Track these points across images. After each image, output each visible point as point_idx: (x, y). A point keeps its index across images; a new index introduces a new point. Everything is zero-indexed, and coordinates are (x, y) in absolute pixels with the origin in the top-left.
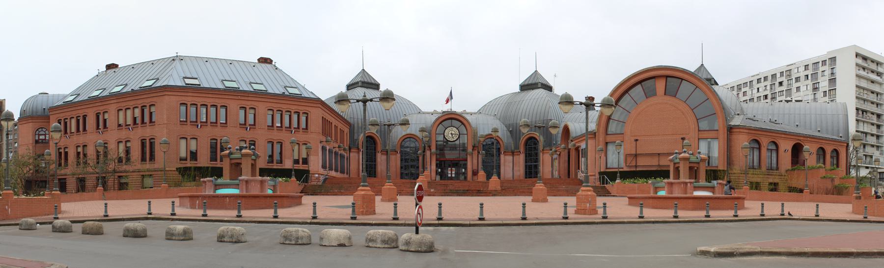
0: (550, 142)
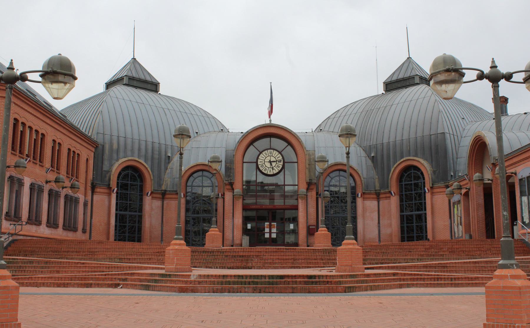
0: (443, 175)
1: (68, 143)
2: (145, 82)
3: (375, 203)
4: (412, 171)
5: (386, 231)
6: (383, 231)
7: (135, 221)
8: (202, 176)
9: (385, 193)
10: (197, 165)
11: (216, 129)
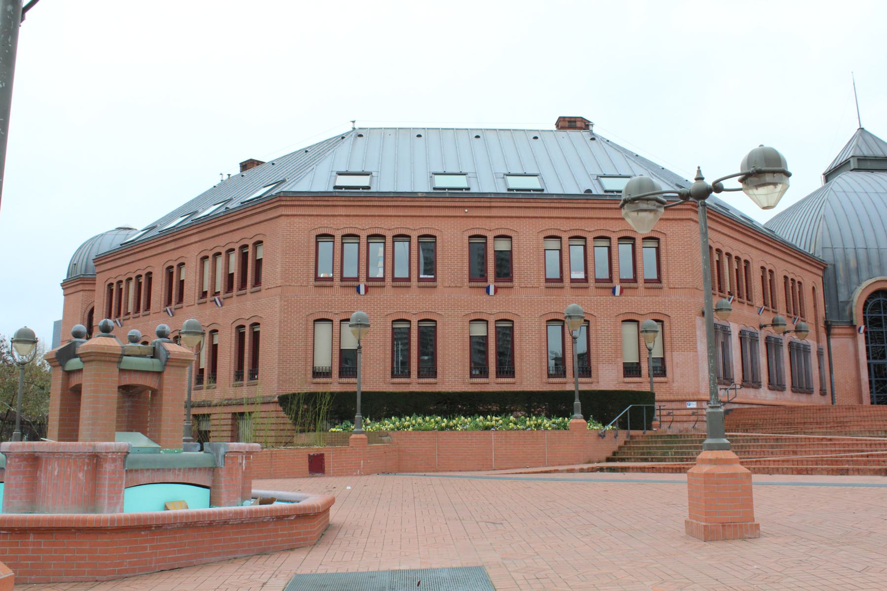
1: (782, 268)
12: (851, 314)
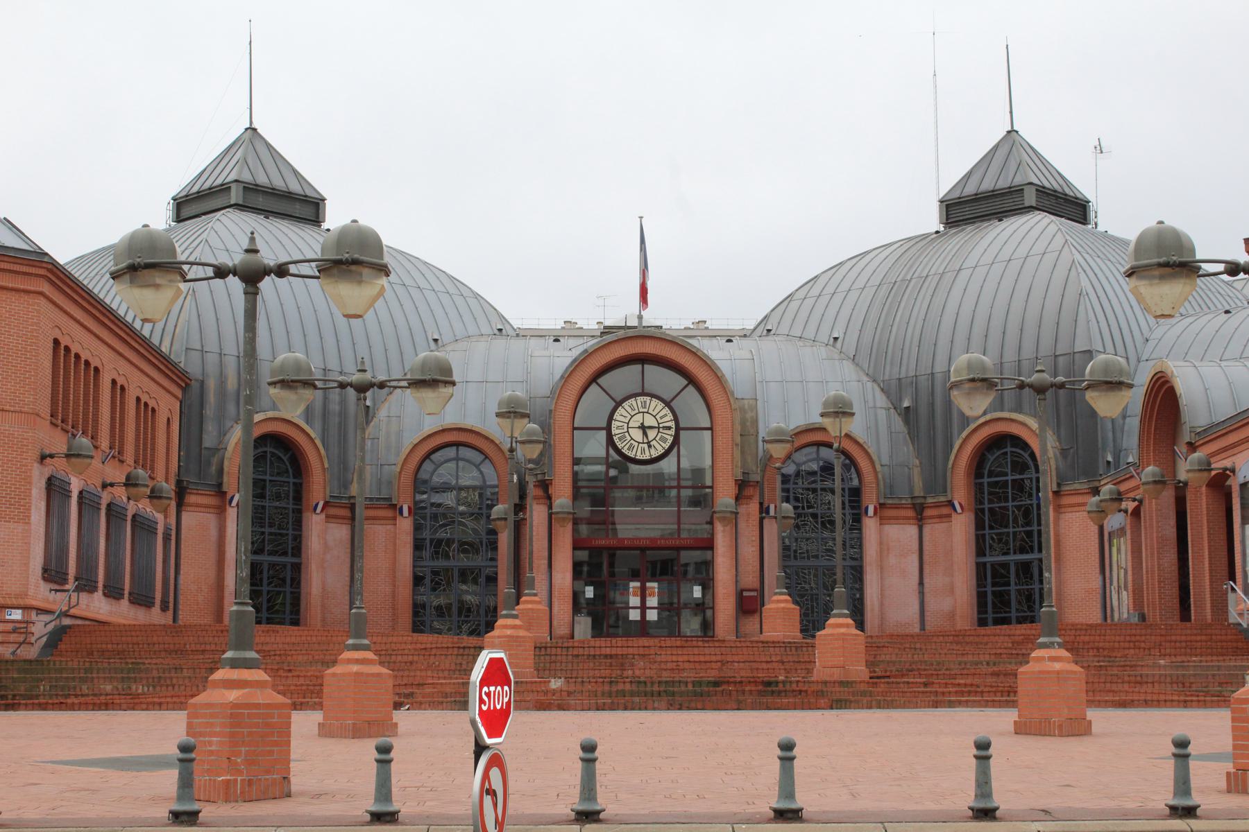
2: (288, 196)
3: (912, 530)
4: (1009, 449)
5: (938, 605)
6: (932, 604)
7: (284, 580)
8: (457, 459)
9: (937, 505)
10: (444, 431)
11: (486, 329)
12: (221, 471)
